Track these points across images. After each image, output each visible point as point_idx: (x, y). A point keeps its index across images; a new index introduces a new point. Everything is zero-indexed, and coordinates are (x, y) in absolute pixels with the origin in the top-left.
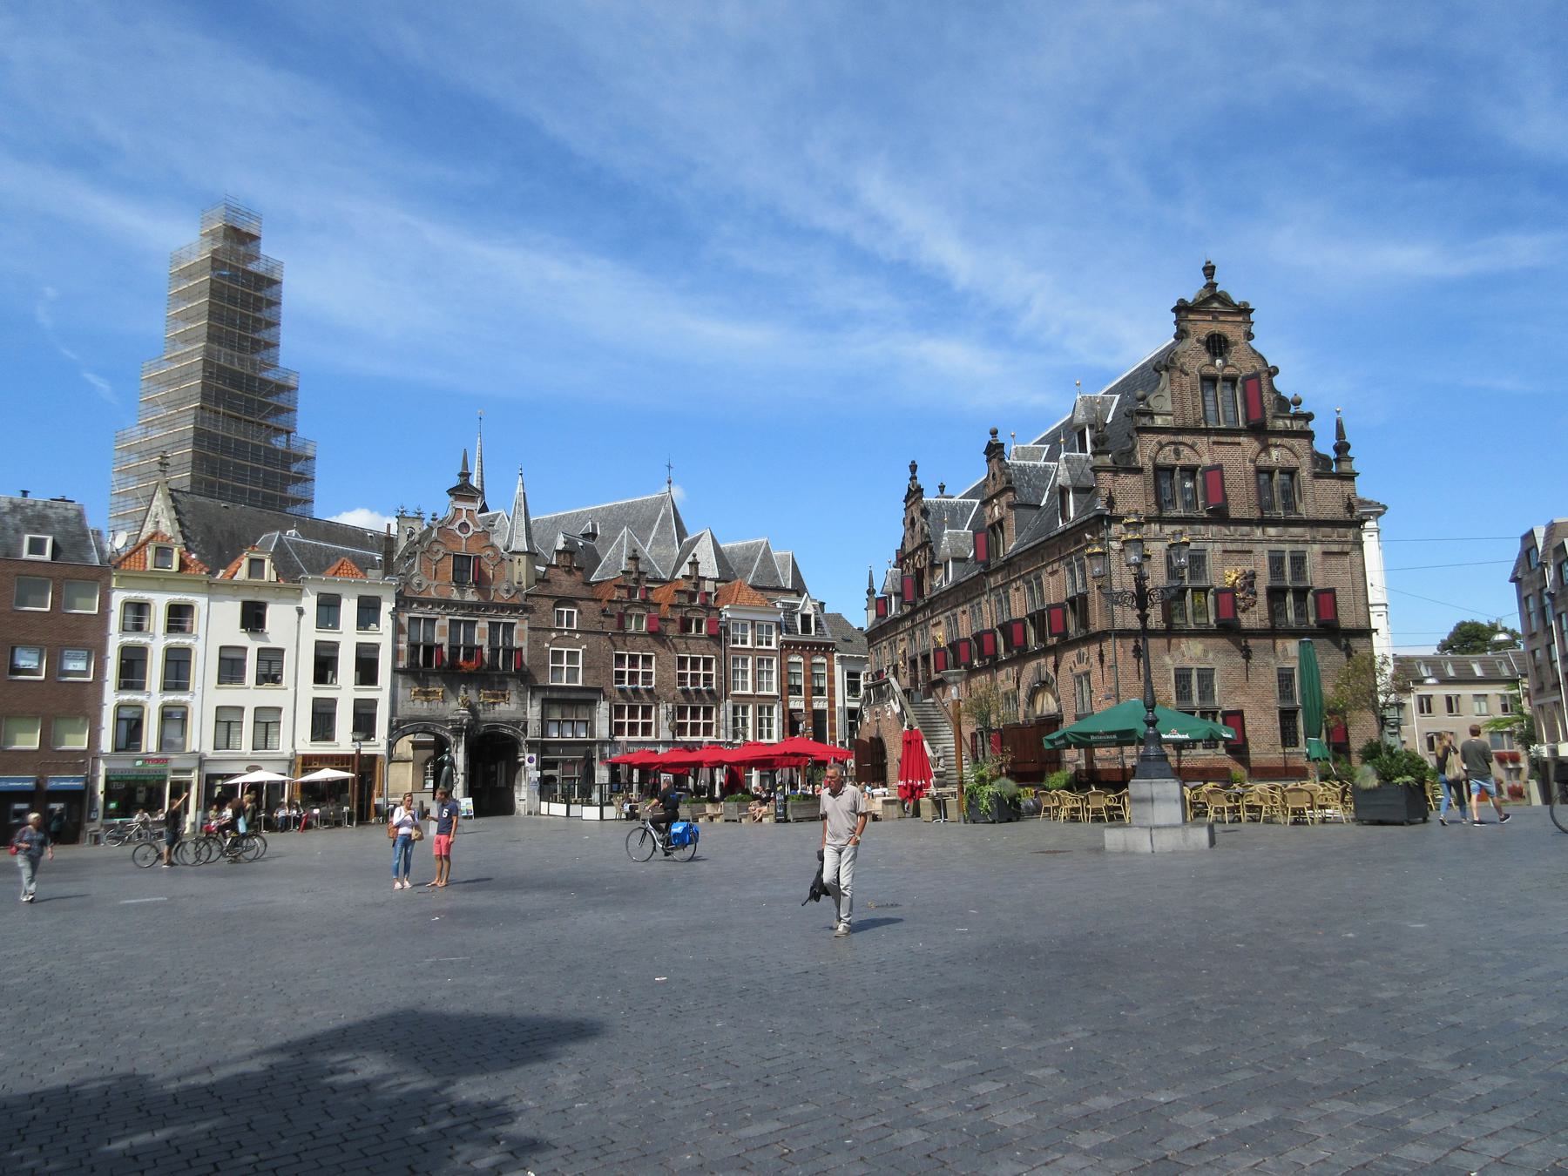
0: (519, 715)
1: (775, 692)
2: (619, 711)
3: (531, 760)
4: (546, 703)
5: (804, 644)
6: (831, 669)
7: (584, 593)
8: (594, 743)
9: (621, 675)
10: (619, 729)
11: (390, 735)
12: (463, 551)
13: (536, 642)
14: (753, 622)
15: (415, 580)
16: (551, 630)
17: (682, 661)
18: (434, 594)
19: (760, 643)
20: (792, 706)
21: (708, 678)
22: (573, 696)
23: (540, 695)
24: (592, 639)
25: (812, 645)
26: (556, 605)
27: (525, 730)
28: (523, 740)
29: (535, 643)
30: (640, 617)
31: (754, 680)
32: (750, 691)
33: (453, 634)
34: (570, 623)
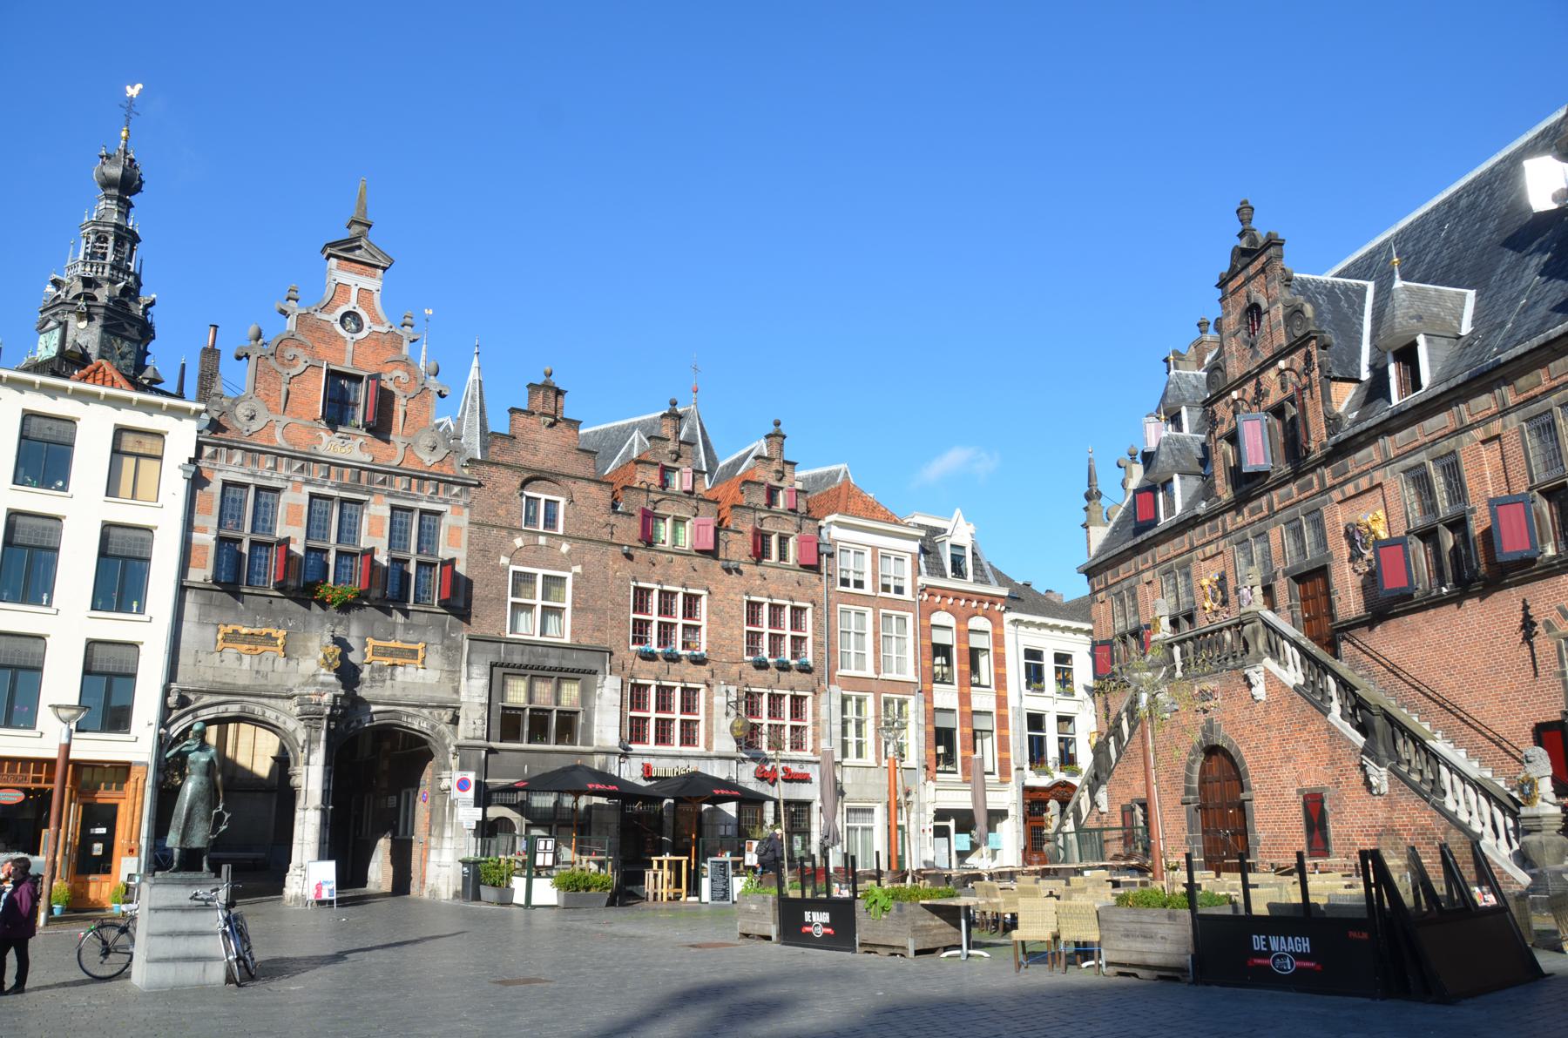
0: (444, 694)
1: (910, 675)
2: (637, 695)
3: (463, 785)
4: (500, 672)
5: (958, 594)
6: (999, 641)
7: (580, 470)
8: (592, 753)
9: (641, 628)
10: (636, 730)
11: (164, 723)
12: (346, 367)
13: (484, 552)
14: (875, 549)
15: (242, 411)
16: (513, 530)
17: (754, 607)
18: (279, 441)
19: (886, 588)
20: (937, 704)
21: (797, 641)
22: (553, 663)
23: (490, 654)
24: (592, 554)
25: (969, 596)
26: (524, 485)
27: (455, 721)
28: (451, 743)
29: (482, 552)
30: (679, 521)
31: (876, 652)
32: (869, 672)
33: (315, 525)
34: (550, 521)
